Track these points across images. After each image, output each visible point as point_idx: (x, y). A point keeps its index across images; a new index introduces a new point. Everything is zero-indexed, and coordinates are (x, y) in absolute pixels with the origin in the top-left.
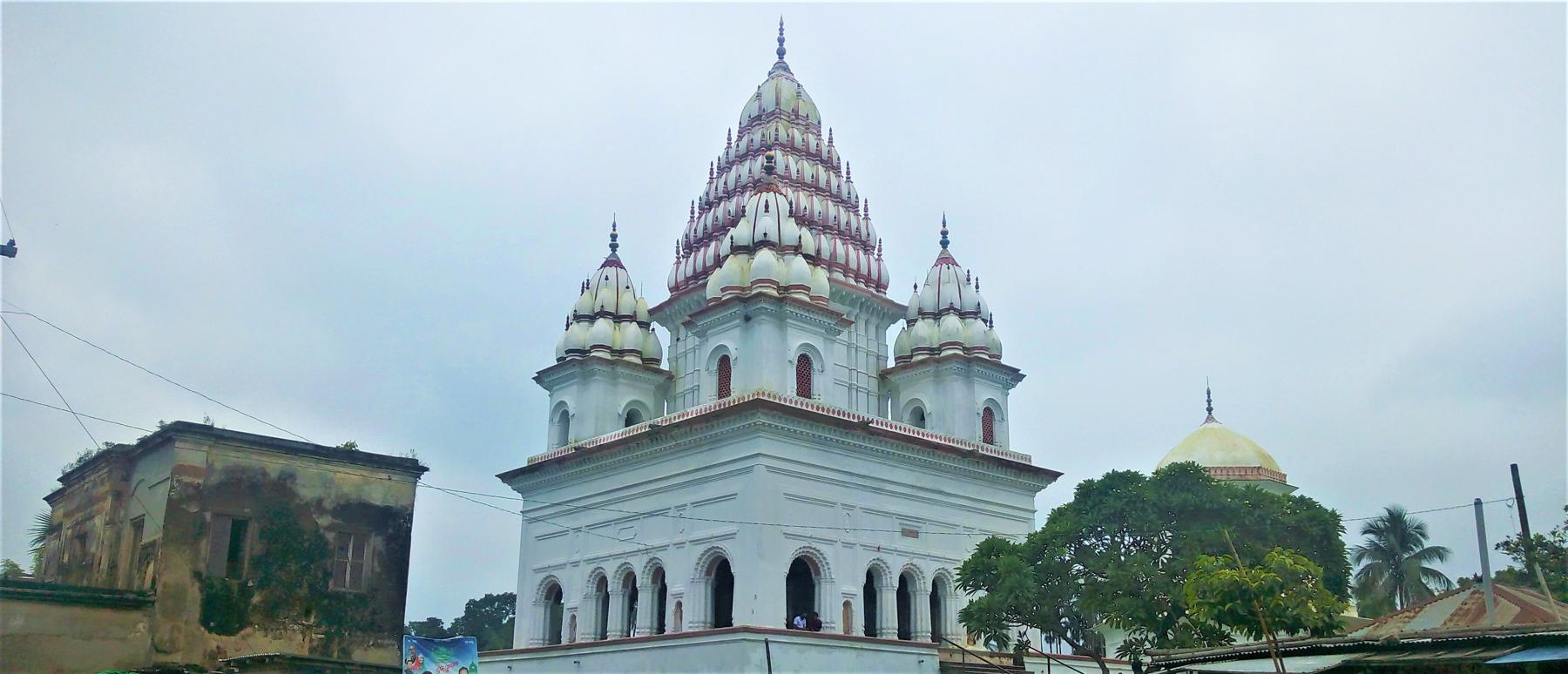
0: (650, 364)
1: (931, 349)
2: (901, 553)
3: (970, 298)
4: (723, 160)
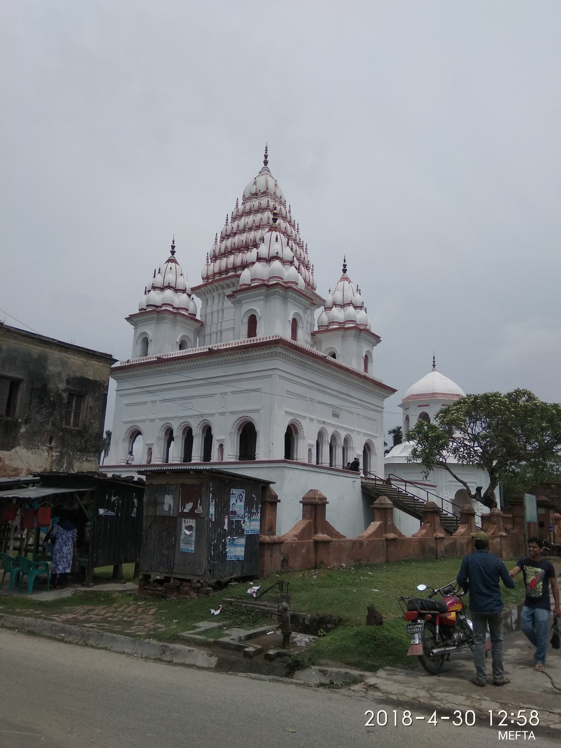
0: (192, 317)
1: (340, 323)
2: (333, 425)
3: (358, 299)
4: (235, 214)
